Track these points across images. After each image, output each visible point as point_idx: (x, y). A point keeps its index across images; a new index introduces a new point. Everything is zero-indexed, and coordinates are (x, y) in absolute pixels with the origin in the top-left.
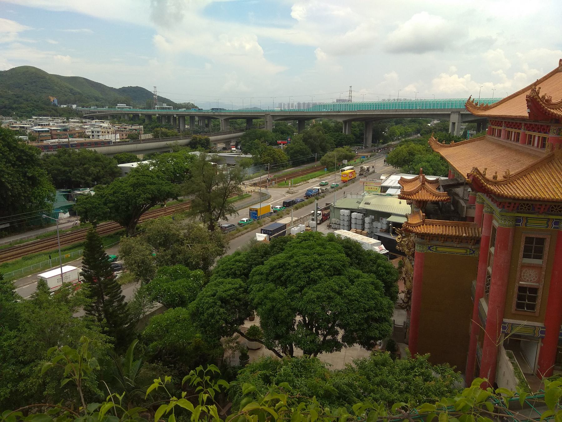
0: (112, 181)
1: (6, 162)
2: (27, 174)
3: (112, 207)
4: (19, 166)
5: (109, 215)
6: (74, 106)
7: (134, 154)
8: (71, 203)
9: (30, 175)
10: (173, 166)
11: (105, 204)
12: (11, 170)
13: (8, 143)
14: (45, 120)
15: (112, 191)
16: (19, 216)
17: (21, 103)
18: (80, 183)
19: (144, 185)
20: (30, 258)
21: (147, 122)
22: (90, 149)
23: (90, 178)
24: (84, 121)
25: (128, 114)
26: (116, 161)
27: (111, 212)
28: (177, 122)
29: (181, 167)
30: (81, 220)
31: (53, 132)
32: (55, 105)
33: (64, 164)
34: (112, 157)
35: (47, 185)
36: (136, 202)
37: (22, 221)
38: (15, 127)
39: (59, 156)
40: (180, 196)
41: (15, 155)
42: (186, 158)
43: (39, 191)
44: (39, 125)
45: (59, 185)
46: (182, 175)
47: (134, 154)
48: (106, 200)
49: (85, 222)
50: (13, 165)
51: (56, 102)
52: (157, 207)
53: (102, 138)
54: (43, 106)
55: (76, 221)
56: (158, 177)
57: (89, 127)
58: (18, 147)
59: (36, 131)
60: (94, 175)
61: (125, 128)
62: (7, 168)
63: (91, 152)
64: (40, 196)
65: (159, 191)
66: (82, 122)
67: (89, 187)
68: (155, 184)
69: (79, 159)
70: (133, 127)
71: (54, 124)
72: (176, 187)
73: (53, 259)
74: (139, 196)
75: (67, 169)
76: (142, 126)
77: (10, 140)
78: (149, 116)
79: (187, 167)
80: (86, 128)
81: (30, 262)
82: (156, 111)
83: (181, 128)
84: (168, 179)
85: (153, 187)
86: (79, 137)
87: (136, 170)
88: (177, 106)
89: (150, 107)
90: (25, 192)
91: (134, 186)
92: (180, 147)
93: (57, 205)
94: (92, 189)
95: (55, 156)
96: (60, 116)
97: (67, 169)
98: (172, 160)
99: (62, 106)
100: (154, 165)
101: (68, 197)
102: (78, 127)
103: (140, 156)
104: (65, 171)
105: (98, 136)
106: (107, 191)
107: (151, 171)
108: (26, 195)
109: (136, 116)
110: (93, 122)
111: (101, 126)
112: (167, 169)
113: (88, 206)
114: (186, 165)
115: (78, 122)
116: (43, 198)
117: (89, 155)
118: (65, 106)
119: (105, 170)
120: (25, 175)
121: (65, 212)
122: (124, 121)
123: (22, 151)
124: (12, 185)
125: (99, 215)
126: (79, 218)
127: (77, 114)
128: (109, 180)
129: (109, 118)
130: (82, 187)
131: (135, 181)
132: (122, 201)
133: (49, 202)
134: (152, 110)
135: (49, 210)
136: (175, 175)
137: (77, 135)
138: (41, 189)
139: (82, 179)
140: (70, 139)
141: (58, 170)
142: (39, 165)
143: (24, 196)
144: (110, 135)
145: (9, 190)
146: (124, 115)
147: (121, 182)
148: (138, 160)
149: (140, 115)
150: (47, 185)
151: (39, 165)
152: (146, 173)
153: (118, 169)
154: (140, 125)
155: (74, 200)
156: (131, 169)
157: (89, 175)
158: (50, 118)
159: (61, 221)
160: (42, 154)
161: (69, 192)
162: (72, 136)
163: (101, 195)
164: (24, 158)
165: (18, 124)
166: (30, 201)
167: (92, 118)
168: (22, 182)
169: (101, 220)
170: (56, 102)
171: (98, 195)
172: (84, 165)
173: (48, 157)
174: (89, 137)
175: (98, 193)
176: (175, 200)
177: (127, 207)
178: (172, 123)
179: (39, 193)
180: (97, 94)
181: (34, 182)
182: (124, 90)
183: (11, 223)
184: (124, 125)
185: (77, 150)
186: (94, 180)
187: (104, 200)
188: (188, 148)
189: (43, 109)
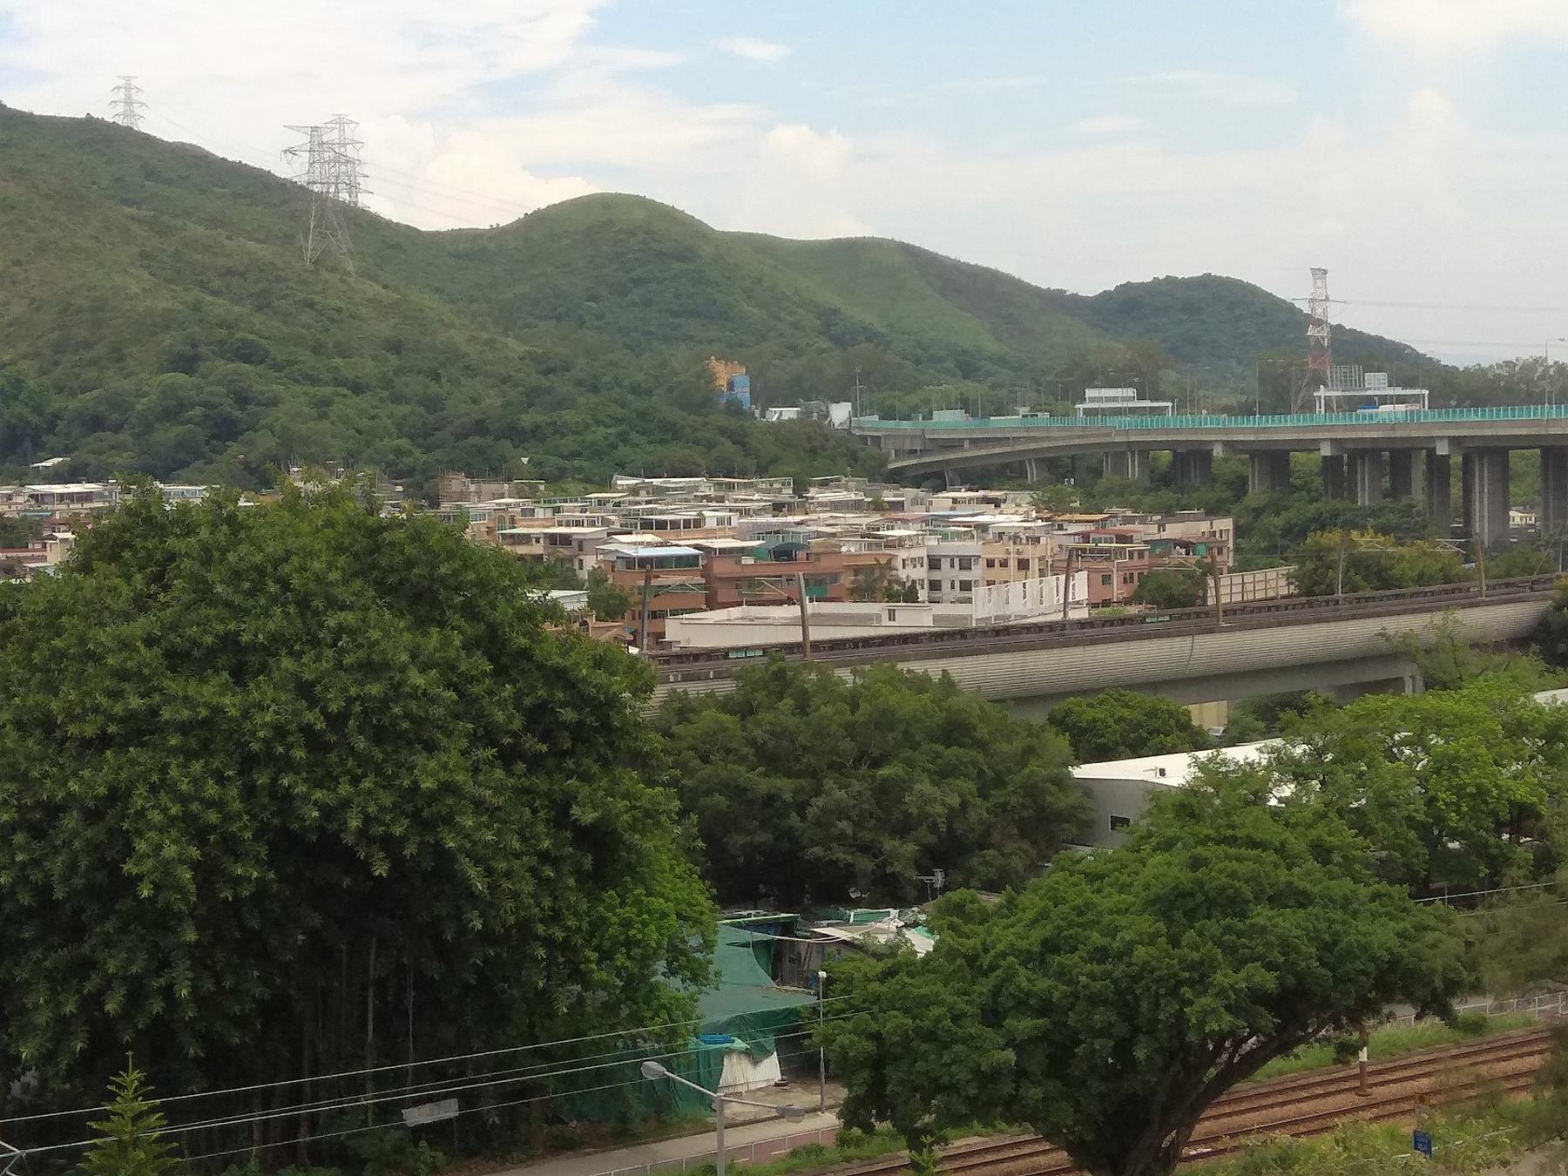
0: (1035, 868)
1: (473, 738)
2: (575, 811)
3: (1033, 1041)
4: (535, 762)
5: (1008, 1088)
6: (840, 413)
7: (1168, 701)
8: (794, 998)
9: (589, 817)
10: (1423, 780)
11: (992, 1016)
12: (493, 786)
13: (493, 629)
14: (683, 497)
15: (1037, 935)
16: (511, 1060)
17: (561, 404)
18: (850, 876)
19: (1234, 905)
21: (1257, 493)
22: (918, 667)
23: (910, 848)
24: (889, 496)
25: (1144, 450)
26: (1060, 744)
27: (1021, 1074)
28: (1456, 490)
29: (1481, 793)
30: (853, 1114)
31: (722, 568)
32: (735, 409)
33: (769, 759)
34: (1038, 717)
35: (672, 877)
36: (1180, 1017)
37: (522, 1091)
38: (525, 539)
39: (745, 710)
40: (1477, 989)
41: (518, 698)
42: (1517, 729)
43: (629, 912)
44: (647, 526)
45: (735, 884)
46: (1479, 849)
47: (1168, 701)
48: (996, 992)
49: (868, 1129)
50: (507, 757)
51: (743, 393)
52: (1310, 1057)
53: (983, 608)
54: (675, 415)
55: (819, 1117)
56: (1321, 852)
57: (917, 529)
58: (538, 654)
59: (630, 562)
60: (934, 828)
61: (1123, 538)
62: (476, 770)
63: (920, 684)
64: (629, 943)
65: (1326, 947)
66: (877, 506)
67: (901, 902)
68: (1302, 900)
69: (851, 730)
70: (1174, 531)
71: (725, 519)
72: (1444, 931)
74: (1200, 977)
75: (784, 786)
76: (1225, 524)
77: (502, 612)
78: (1274, 459)
79: (1521, 793)
80: (900, 543)
82: (1318, 424)
83: (1482, 527)
84: (1384, 870)
85: (1288, 922)
86: (862, 593)
87: (1185, 805)
88: (1455, 388)
89: (1278, 403)
90: (555, 917)
91: (1178, 907)
92: (1474, 660)
93: (715, 1005)
95: (726, 705)
96: (762, 471)
97: (784, 786)
98: (1418, 742)
99: (774, 414)
100: (1299, 773)
101: (779, 960)
102: (852, 532)
103: (1210, 715)
104: (770, 799)
105: (966, 586)
106: (1005, 936)
107: (1275, 814)
108: (560, 934)
109: (1192, 458)
110: (942, 502)
111: (983, 528)
112: (1384, 805)
113: (894, 1022)
114: (1517, 778)
115: (856, 506)
116: (645, 960)
117: (907, 704)
118: (789, 413)
119: (998, 796)
120: (560, 814)
121: (755, 1055)
122: (1120, 494)
123: (560, 677)
124: (489, 872)
125: (950, 1088)
126: (842, 1093)
127: (853, 458)
128: (1017, 862)
129: (1033, 475)
130: (856, 904)
131: (1186, 878)
132: (1095, 1001)
133: (675, 982)
134: (1290, 421)
135: (673, 1034)
136: (1433, 844)
137: (847, 580)
138: (637, 901)
139: (865, 849)
140: (812, 607)
141: (737, 791)
142: (640, 760)
143: (549, 942)
144: (1033, 582)
145: (472, 897)
146: (1119, 453)
147: (1093, 877)
148: (1194, 740)
149: (1218, 451)
150: (672, 877)
151: (640, 760)
152: (1247, 823)
153: (1074, 798)
154: (1213, 511)
155: (808, 981)
156: (1155, 795)
157: (903, 830)
158: (704, 486)
159: (734, 1109)
160: (661, 692)
161: (787, 928)
162: (821, 587)
163: (971, 960)
164: (568, 715)
165: (540, 524)
167: (934, 479)
168: (544, 857)
169: (959, 1121)
170: (743, 393)
171: (952, 954)
172: (877, 764)
173: (683, 710)
174: (910, 596)
175: (951, 940)
176: (1433, 1023)
177: (1123, 1048)
178: (1418, 494)
179: (627, 924)
180: (973, 333)
181: (603, 855)
182: (1129, 306)
183: (467, 1099)
184: (1119, 520)
185: (845, 674)
186: (933, 858)
187: (985, 986)
188: (1527, 663)
189: (672, 432)
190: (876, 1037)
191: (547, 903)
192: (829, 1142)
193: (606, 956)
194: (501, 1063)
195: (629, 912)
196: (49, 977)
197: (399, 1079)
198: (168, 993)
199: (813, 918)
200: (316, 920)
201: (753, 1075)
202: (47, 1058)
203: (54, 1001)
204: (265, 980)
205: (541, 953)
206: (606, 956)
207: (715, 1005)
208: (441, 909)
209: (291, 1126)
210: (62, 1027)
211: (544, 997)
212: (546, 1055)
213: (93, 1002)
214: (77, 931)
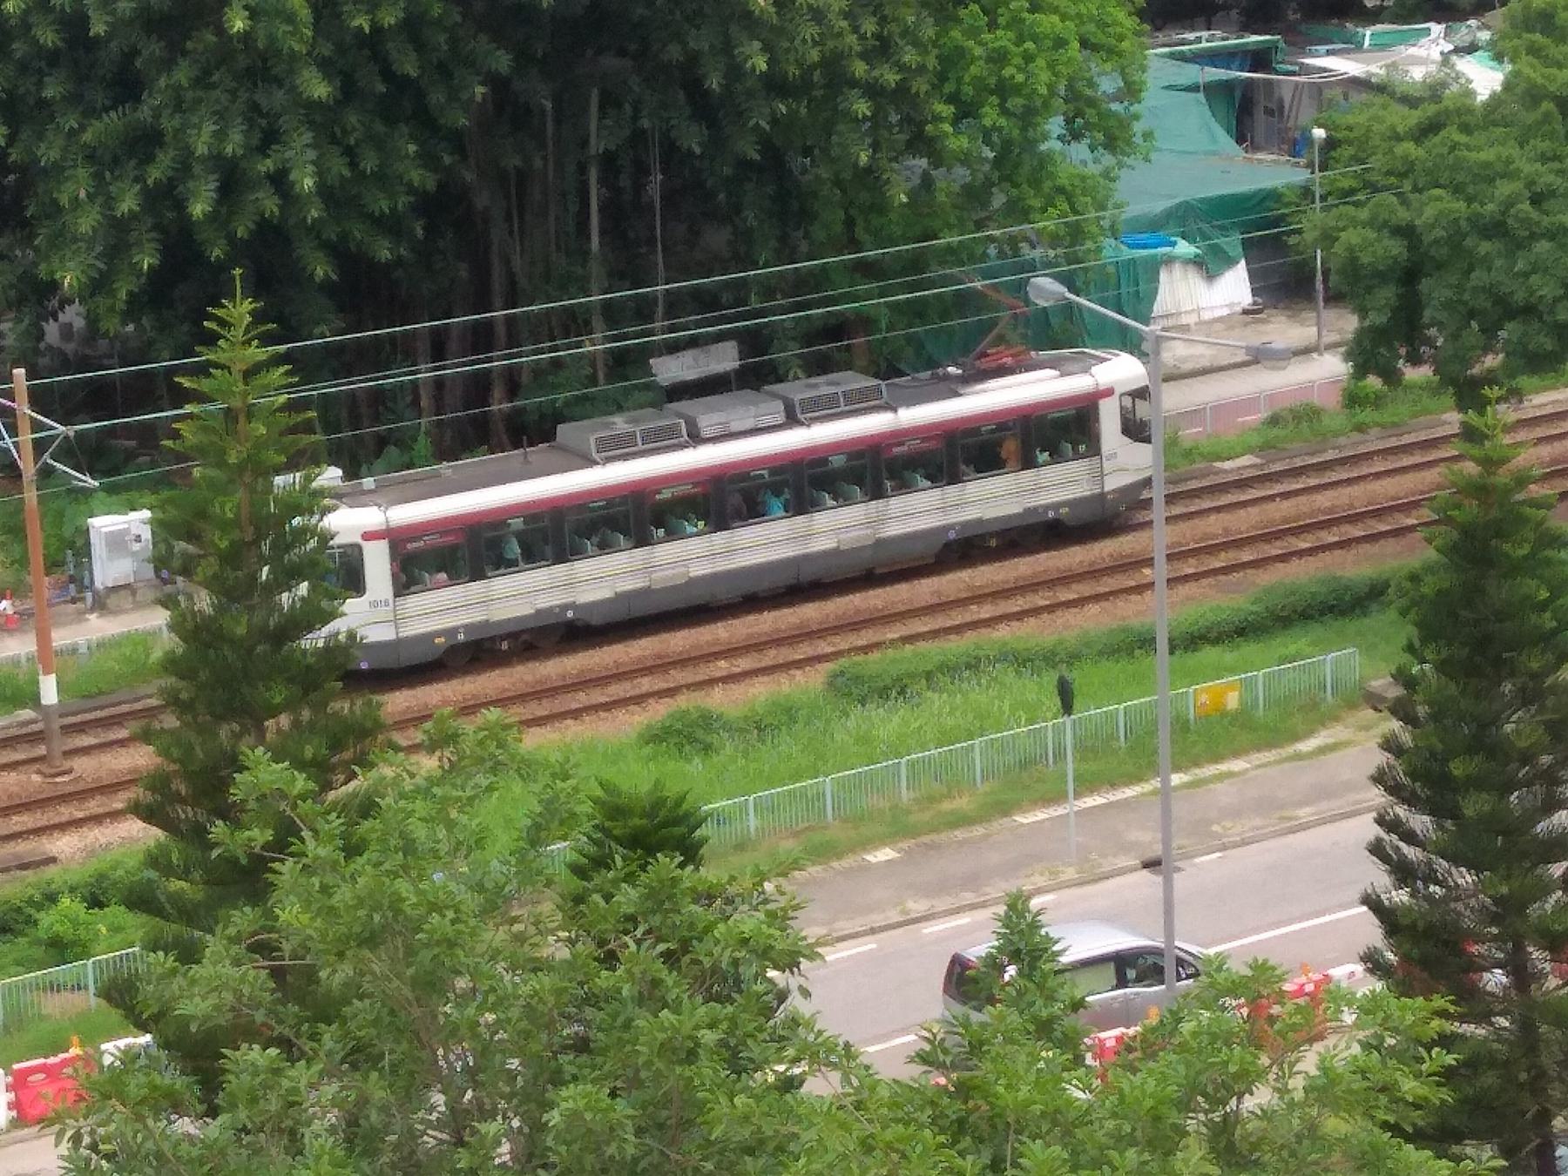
8: (1271, 172)
16: (818, 280)
20: (894, 689)
30: (1368, 355)
43: (1003, 38)
49: (1391, 377)
55: (1312, 361)
64: (1003, 90)
73: (1088, 712)
81: (886, 721)
90: (881, 49)
93: (1145, 188)
94: (1474, 30)
101: (1245, 113)
108: (891, 78)
113: (1435, 209)
116: (1029, 117)
121: (1210, 266)
125: (1529, 311)
126: (1346, 323)
130: (1374, 16)
133: (1080, 150)
135: (1076, 233)
138: (1015, 22)
143: (873, 91)
155: (1296, 146)
161: (1260, 59)
166: (921, 143)
171: (1533, 96)
175: (1534, 72)
179: (998, 58)
190: (1406, 232)
191: (869, 26)
192: (1332, 401)
193: (966, 111)
194: (802, 283)
195: (1003, 38)
196: (91, 157)
197: (643, 311)
198: (280, 181)
199: (1301, 41)
200: (502, 61)
201: (1208, 297)
202: (98, 286)
203: (102, 193)
204: (428, 159)
205: (862, 107)
206: (966, 111)
207: (1145, 188)
208: (701, 40)
209: (479, 388)
210: (118, 237)
211: (870, 178)
212: (867, 270)
213: (165, 198)
214: (128, 87)
